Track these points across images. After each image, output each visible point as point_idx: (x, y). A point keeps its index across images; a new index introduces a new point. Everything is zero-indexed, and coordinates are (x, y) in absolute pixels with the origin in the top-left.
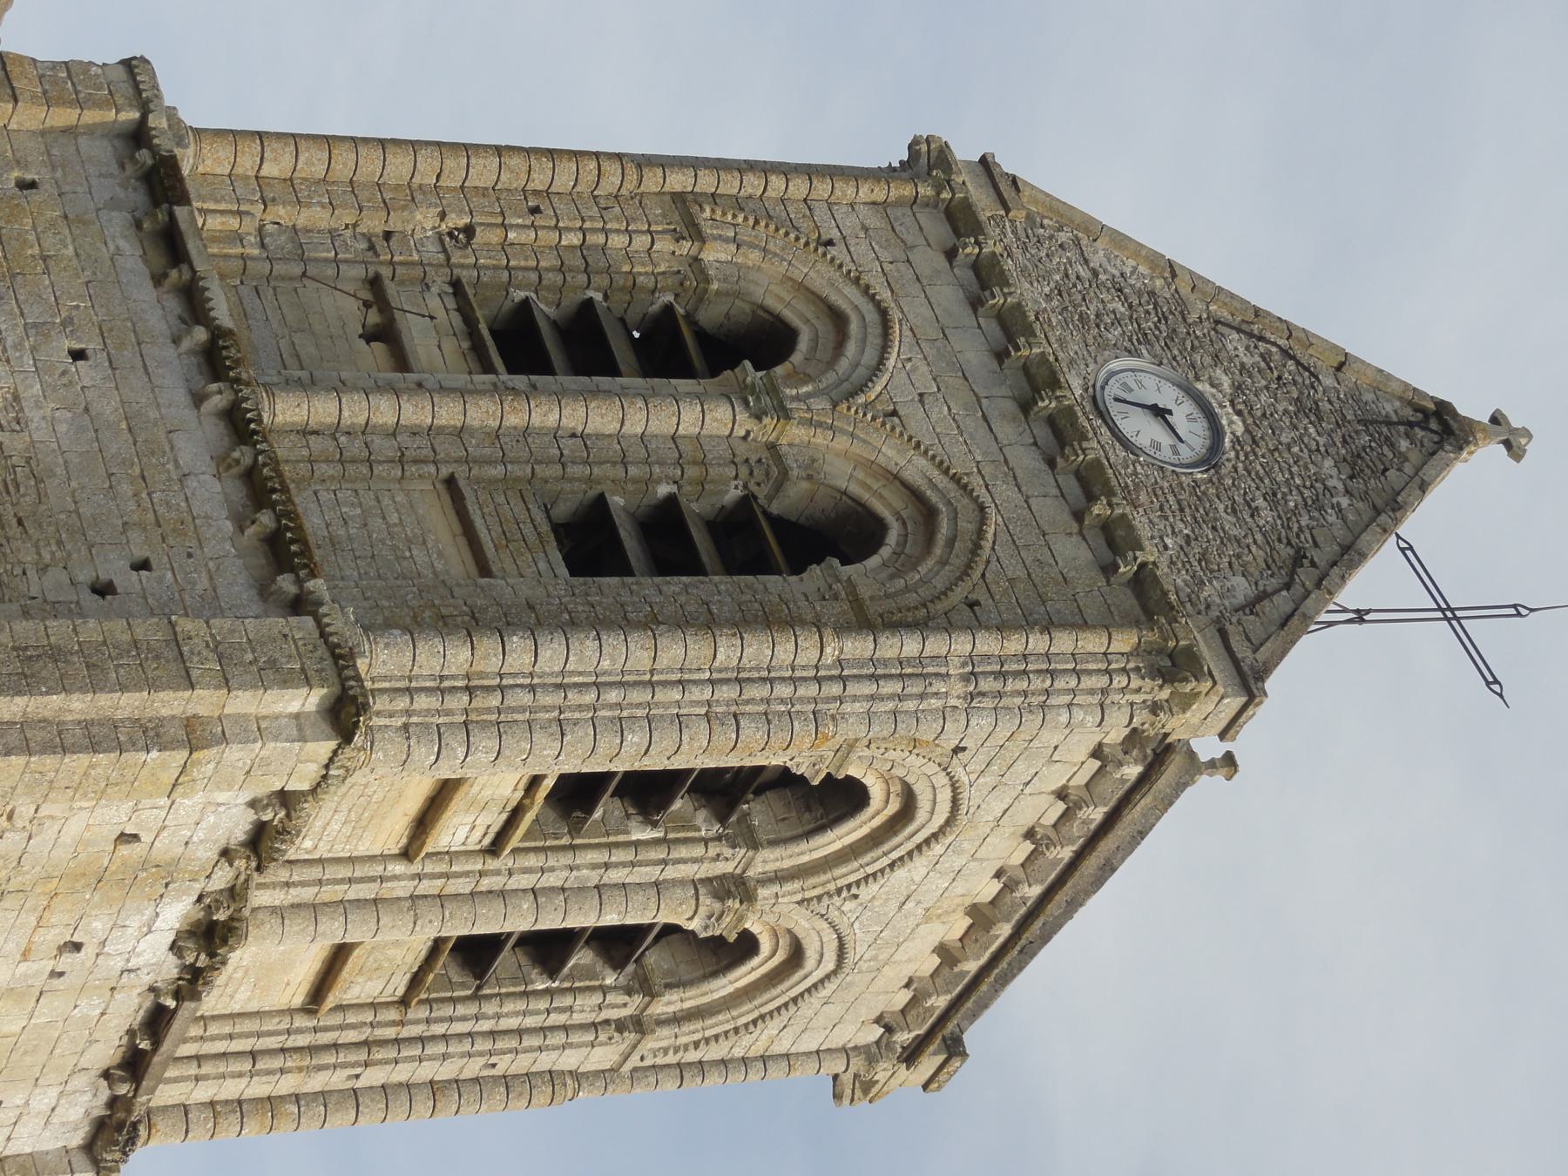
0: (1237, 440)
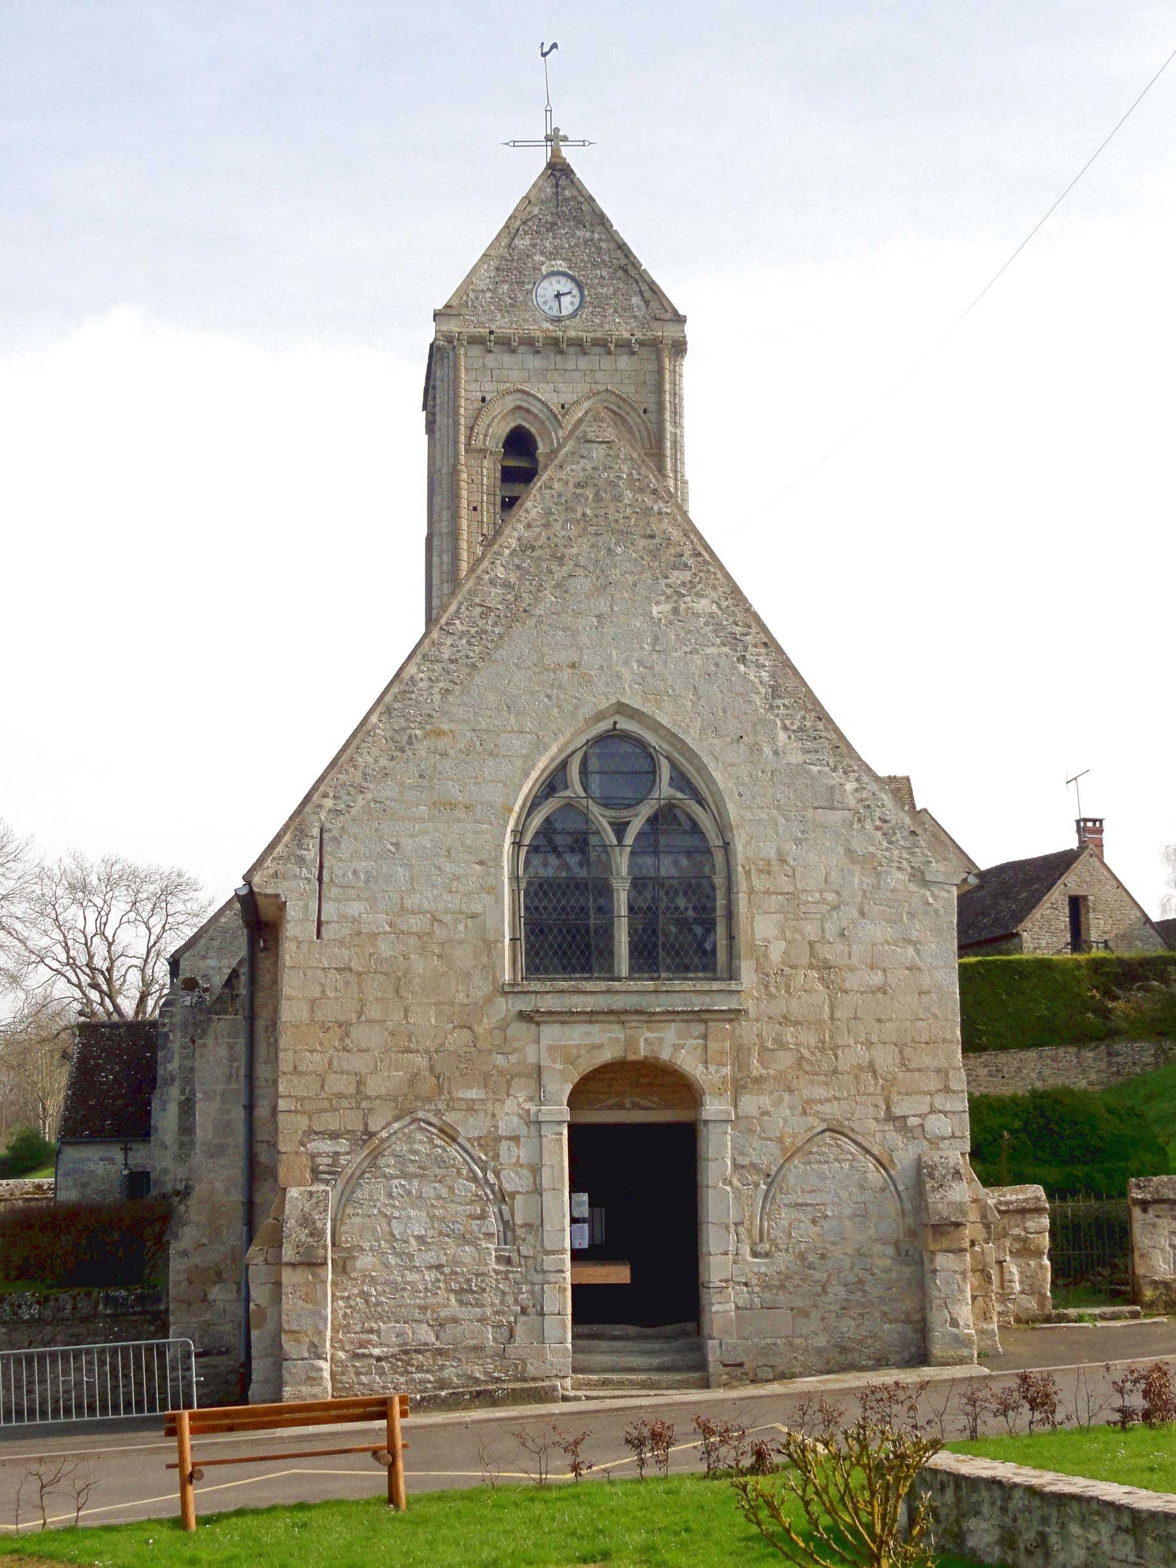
0: (570, 268)
